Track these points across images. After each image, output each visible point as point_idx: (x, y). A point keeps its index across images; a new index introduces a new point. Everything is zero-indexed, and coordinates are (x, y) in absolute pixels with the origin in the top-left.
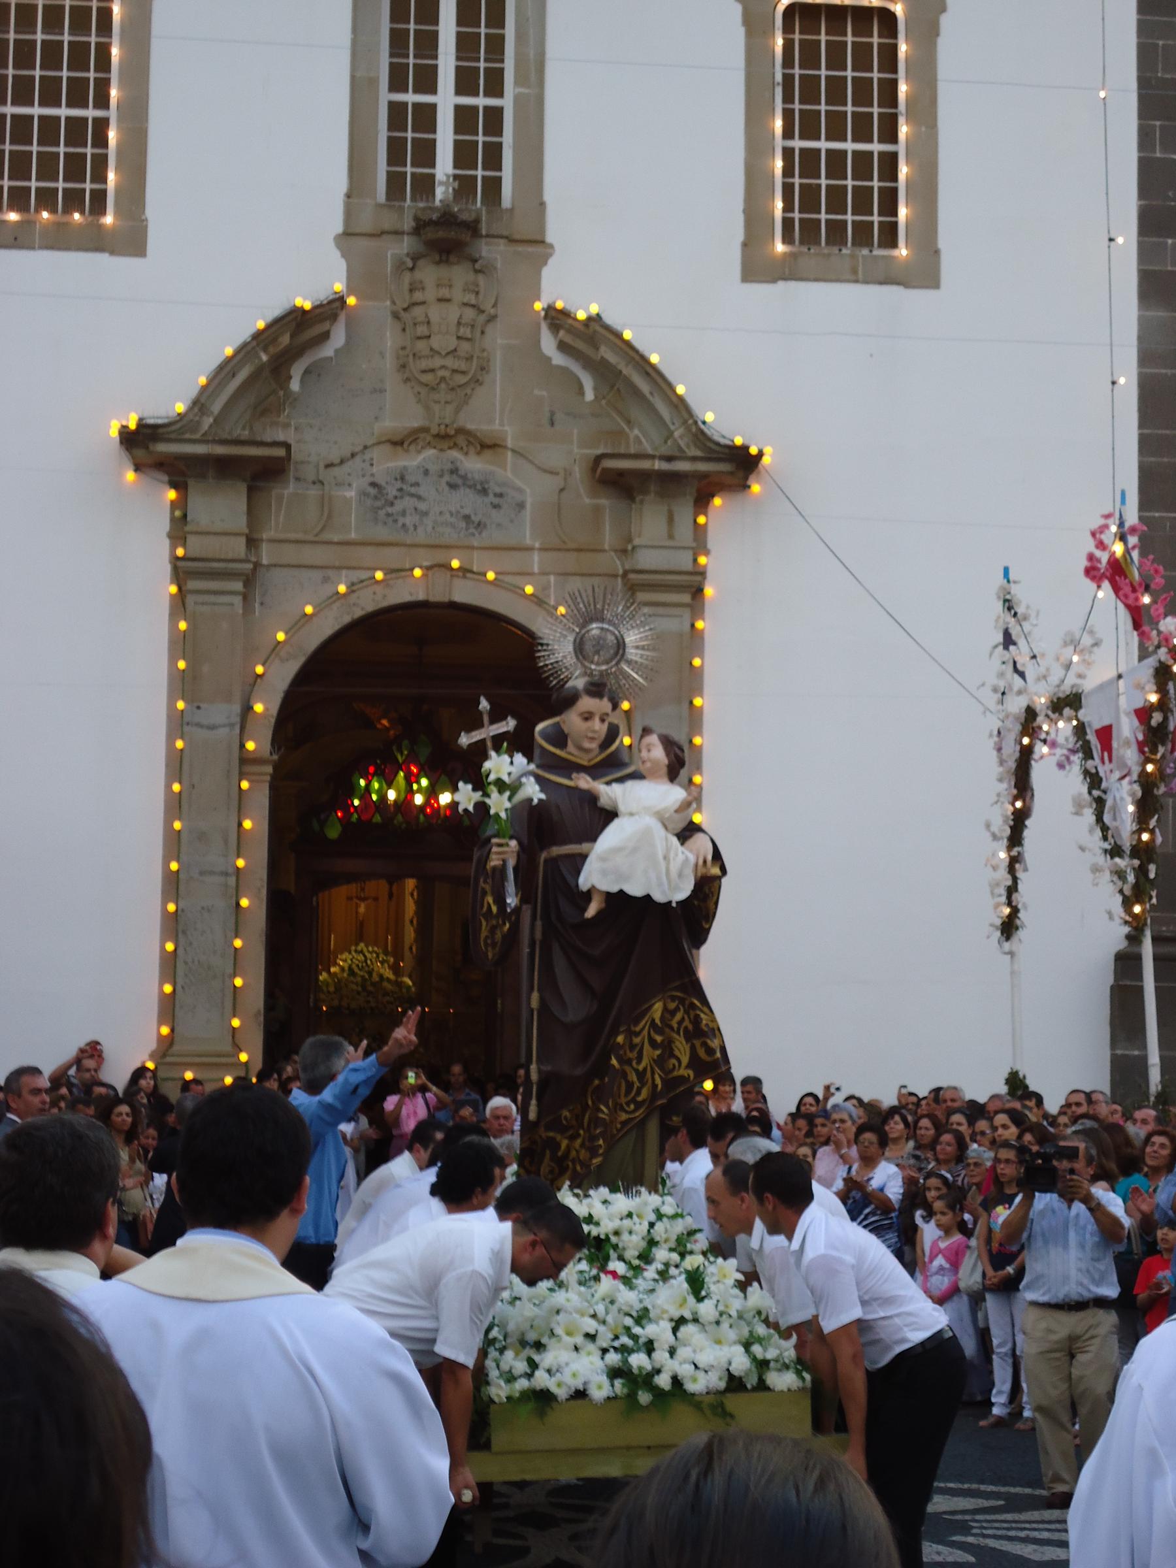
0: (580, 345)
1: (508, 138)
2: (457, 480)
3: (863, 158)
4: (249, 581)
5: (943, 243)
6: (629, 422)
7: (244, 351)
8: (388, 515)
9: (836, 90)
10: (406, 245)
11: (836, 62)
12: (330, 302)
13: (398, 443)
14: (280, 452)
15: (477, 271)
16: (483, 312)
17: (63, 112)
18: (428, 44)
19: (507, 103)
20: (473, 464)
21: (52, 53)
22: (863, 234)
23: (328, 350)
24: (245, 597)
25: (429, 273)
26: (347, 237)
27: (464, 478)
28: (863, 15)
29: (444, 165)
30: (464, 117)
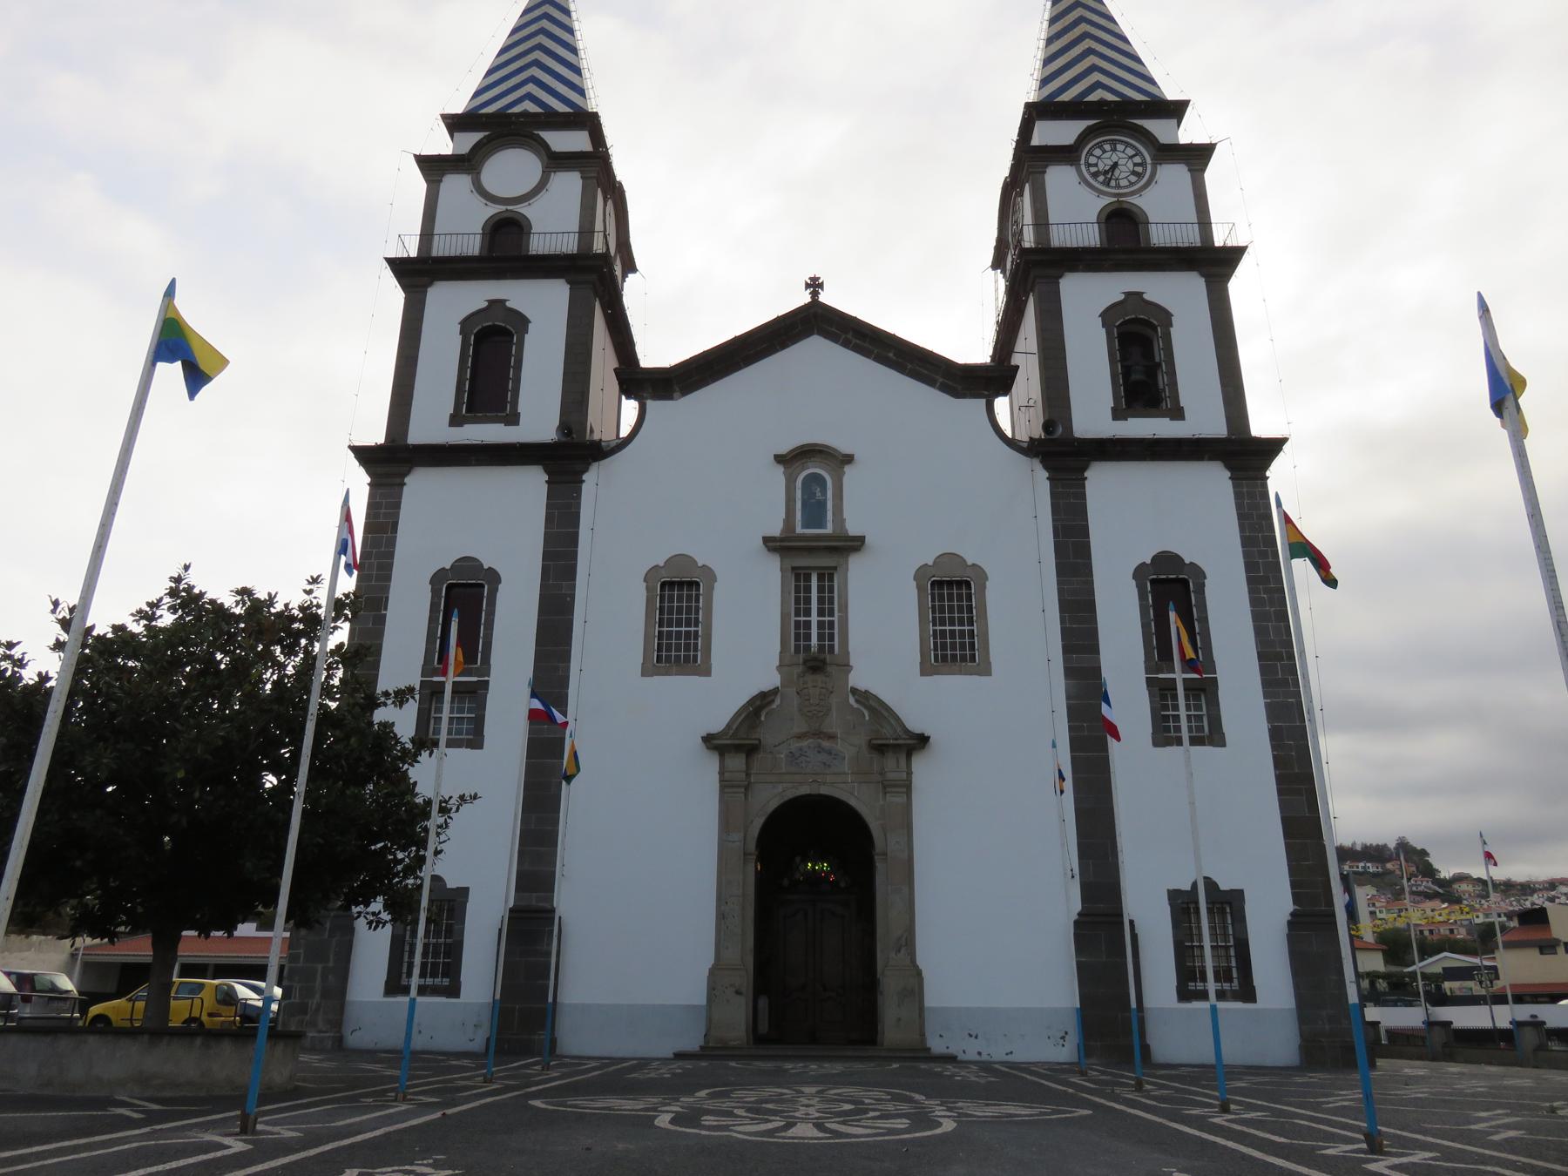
0: (863, 701)
1: (836, 631)
2: (820, 750)
3: (962, 633)
4: (747, 788)
5: (991, 660)
6: (882, 727)
7: (745, 707)
8: (797, 763)
9: (951, 609)
10: (801, 668)
11: (951, 599)
12: (774, 689)
13: (800, 737)
14: (757, 742)
15: (826, 676)
16: (827, 689)
17: (683, 629)
18: (808, 601)
19: (836, 619)
20: (826, 744)
21: (680, 611)
22: (963, 659)
23: (774, 706)
24: (746, 795)
25: (810, 678)
26: (780, 667)
27: (823, 749)
28: (959, 584)
29: (814, 640)
30: (821, 625)
